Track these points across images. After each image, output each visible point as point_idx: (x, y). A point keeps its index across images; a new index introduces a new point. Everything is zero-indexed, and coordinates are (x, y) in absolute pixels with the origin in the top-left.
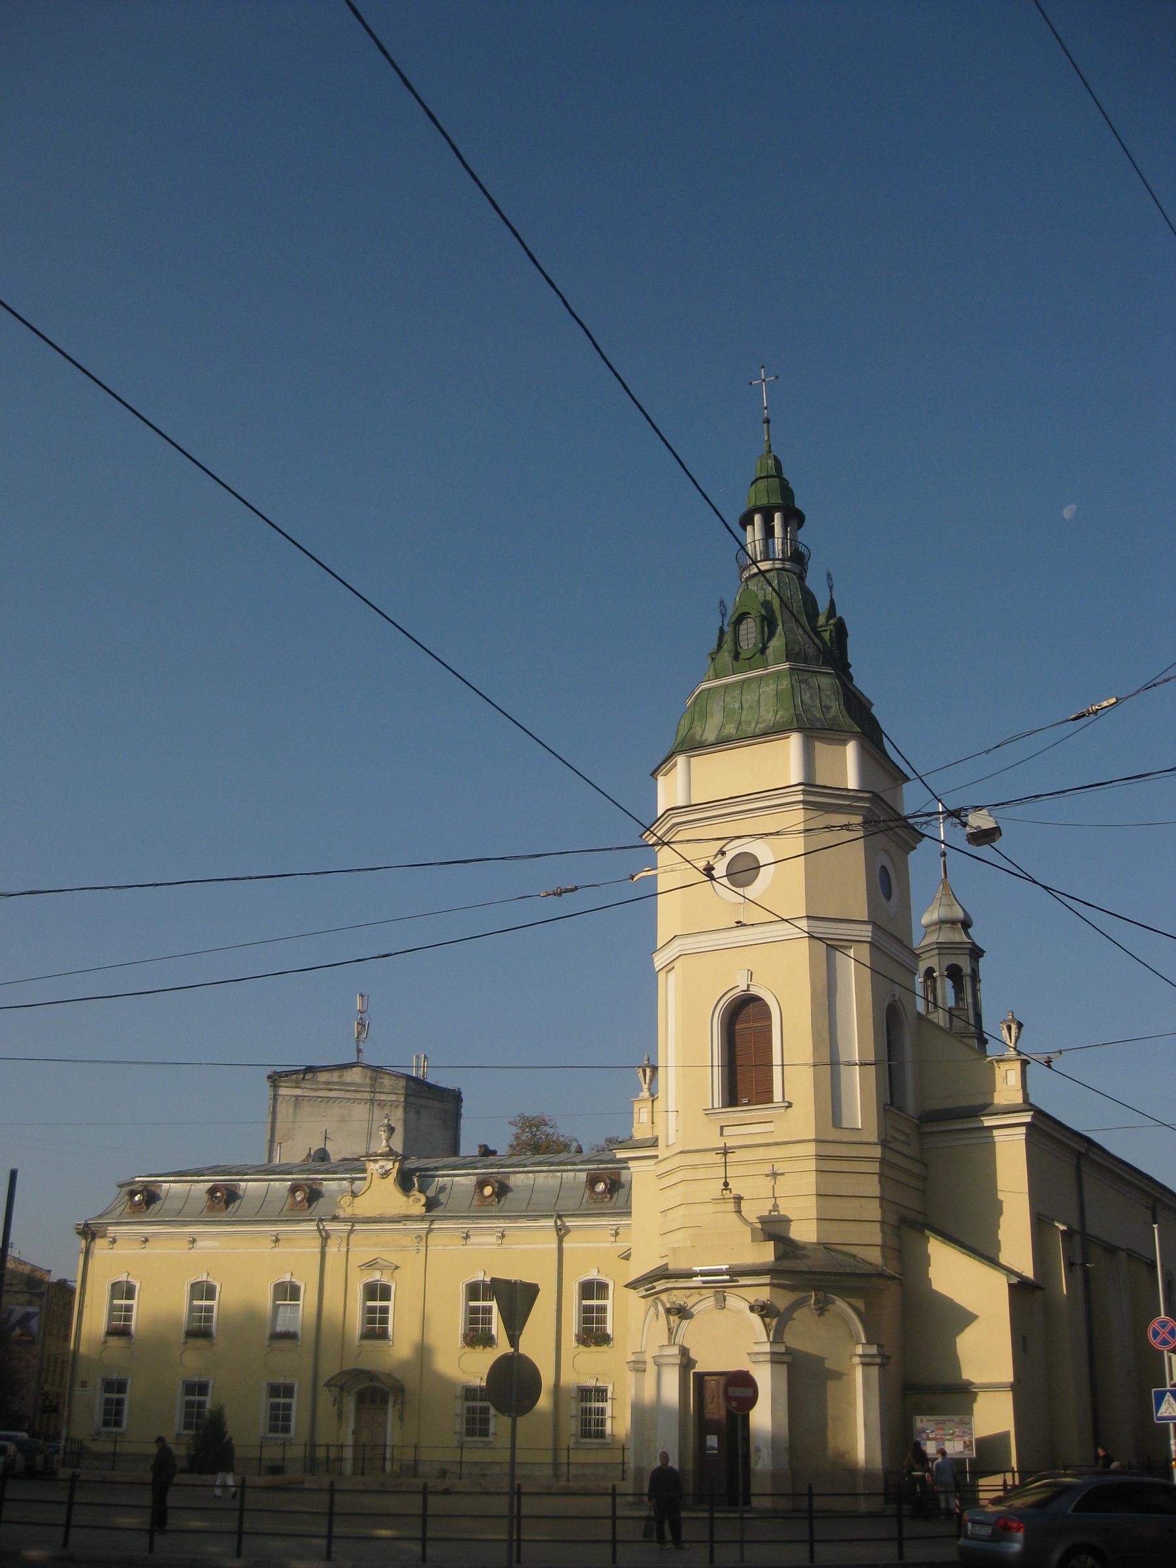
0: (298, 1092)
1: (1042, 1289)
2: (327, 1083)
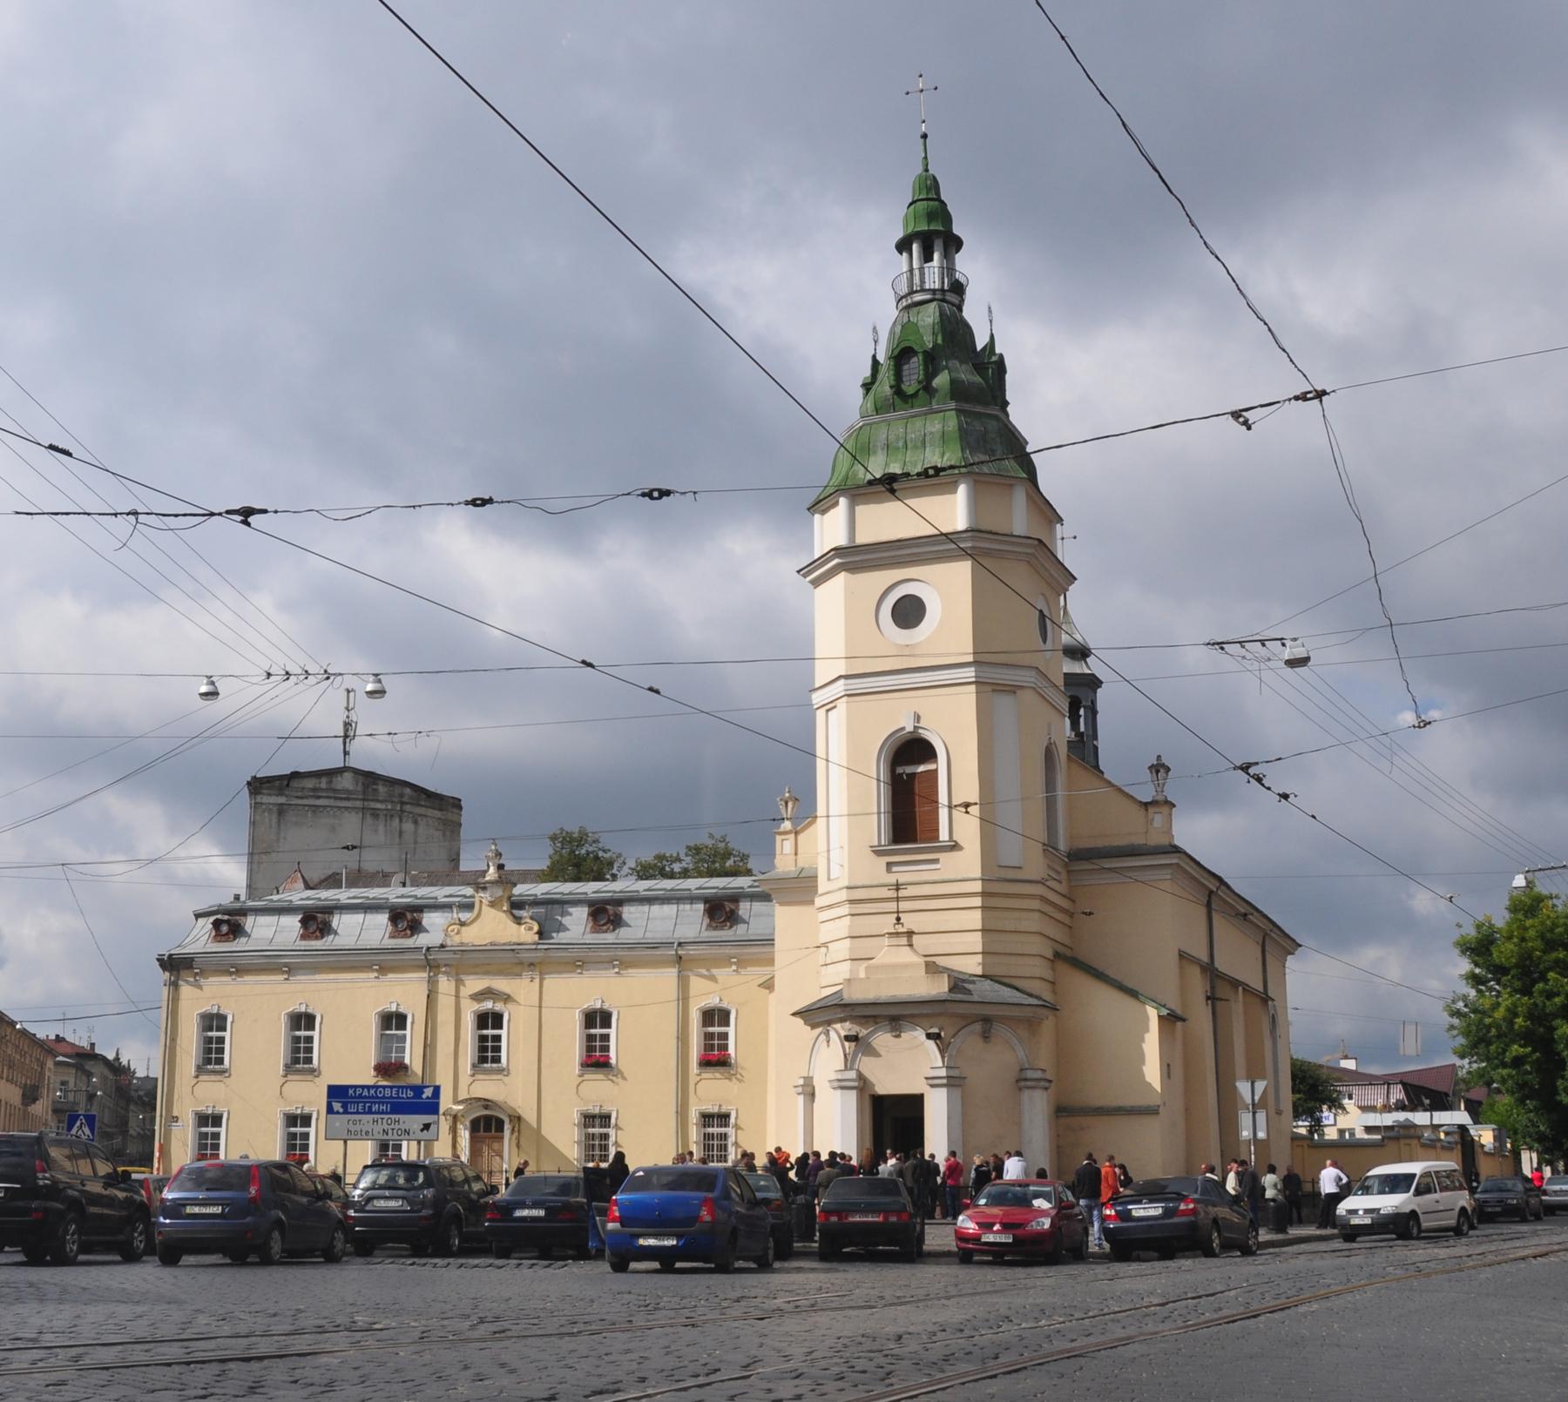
0: (282, 800)
1: (1183, 1020)
2: (314, 790)
